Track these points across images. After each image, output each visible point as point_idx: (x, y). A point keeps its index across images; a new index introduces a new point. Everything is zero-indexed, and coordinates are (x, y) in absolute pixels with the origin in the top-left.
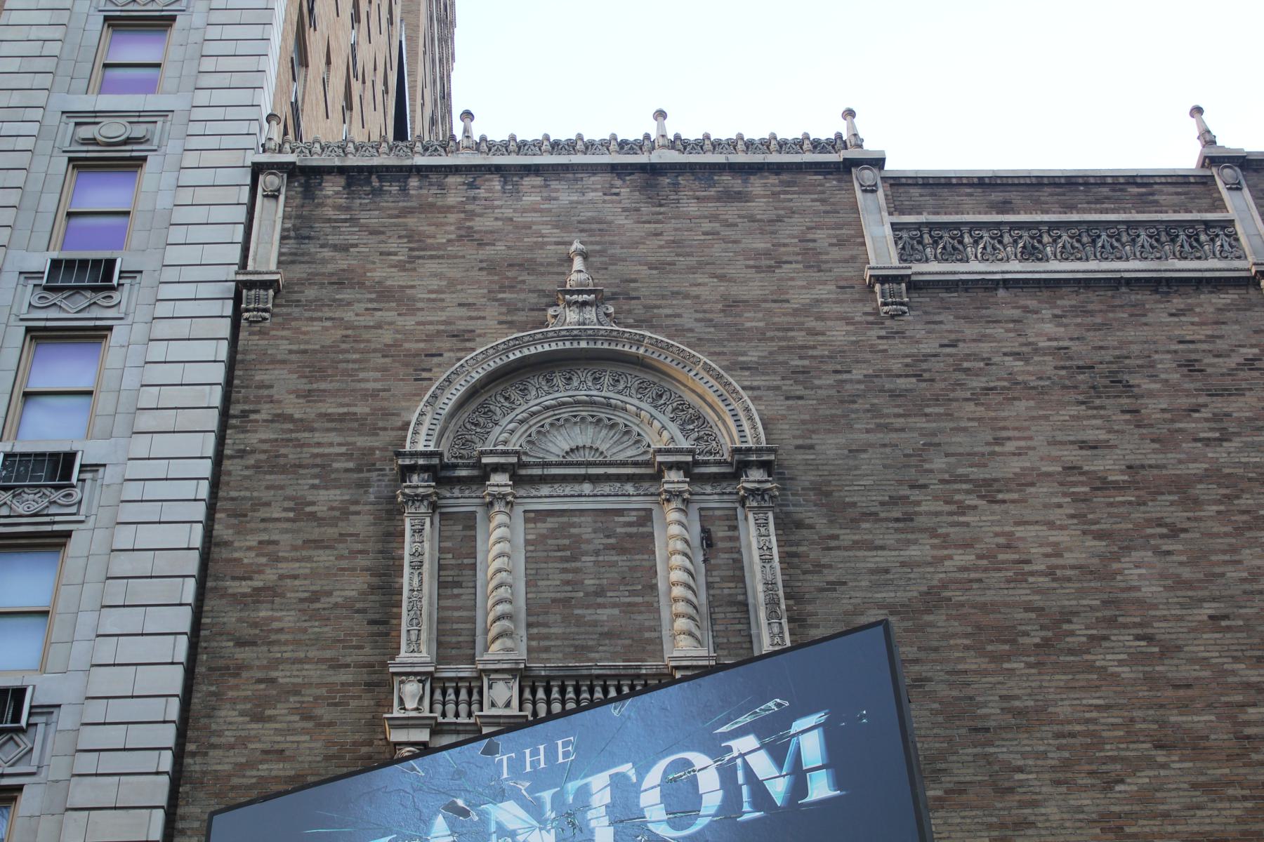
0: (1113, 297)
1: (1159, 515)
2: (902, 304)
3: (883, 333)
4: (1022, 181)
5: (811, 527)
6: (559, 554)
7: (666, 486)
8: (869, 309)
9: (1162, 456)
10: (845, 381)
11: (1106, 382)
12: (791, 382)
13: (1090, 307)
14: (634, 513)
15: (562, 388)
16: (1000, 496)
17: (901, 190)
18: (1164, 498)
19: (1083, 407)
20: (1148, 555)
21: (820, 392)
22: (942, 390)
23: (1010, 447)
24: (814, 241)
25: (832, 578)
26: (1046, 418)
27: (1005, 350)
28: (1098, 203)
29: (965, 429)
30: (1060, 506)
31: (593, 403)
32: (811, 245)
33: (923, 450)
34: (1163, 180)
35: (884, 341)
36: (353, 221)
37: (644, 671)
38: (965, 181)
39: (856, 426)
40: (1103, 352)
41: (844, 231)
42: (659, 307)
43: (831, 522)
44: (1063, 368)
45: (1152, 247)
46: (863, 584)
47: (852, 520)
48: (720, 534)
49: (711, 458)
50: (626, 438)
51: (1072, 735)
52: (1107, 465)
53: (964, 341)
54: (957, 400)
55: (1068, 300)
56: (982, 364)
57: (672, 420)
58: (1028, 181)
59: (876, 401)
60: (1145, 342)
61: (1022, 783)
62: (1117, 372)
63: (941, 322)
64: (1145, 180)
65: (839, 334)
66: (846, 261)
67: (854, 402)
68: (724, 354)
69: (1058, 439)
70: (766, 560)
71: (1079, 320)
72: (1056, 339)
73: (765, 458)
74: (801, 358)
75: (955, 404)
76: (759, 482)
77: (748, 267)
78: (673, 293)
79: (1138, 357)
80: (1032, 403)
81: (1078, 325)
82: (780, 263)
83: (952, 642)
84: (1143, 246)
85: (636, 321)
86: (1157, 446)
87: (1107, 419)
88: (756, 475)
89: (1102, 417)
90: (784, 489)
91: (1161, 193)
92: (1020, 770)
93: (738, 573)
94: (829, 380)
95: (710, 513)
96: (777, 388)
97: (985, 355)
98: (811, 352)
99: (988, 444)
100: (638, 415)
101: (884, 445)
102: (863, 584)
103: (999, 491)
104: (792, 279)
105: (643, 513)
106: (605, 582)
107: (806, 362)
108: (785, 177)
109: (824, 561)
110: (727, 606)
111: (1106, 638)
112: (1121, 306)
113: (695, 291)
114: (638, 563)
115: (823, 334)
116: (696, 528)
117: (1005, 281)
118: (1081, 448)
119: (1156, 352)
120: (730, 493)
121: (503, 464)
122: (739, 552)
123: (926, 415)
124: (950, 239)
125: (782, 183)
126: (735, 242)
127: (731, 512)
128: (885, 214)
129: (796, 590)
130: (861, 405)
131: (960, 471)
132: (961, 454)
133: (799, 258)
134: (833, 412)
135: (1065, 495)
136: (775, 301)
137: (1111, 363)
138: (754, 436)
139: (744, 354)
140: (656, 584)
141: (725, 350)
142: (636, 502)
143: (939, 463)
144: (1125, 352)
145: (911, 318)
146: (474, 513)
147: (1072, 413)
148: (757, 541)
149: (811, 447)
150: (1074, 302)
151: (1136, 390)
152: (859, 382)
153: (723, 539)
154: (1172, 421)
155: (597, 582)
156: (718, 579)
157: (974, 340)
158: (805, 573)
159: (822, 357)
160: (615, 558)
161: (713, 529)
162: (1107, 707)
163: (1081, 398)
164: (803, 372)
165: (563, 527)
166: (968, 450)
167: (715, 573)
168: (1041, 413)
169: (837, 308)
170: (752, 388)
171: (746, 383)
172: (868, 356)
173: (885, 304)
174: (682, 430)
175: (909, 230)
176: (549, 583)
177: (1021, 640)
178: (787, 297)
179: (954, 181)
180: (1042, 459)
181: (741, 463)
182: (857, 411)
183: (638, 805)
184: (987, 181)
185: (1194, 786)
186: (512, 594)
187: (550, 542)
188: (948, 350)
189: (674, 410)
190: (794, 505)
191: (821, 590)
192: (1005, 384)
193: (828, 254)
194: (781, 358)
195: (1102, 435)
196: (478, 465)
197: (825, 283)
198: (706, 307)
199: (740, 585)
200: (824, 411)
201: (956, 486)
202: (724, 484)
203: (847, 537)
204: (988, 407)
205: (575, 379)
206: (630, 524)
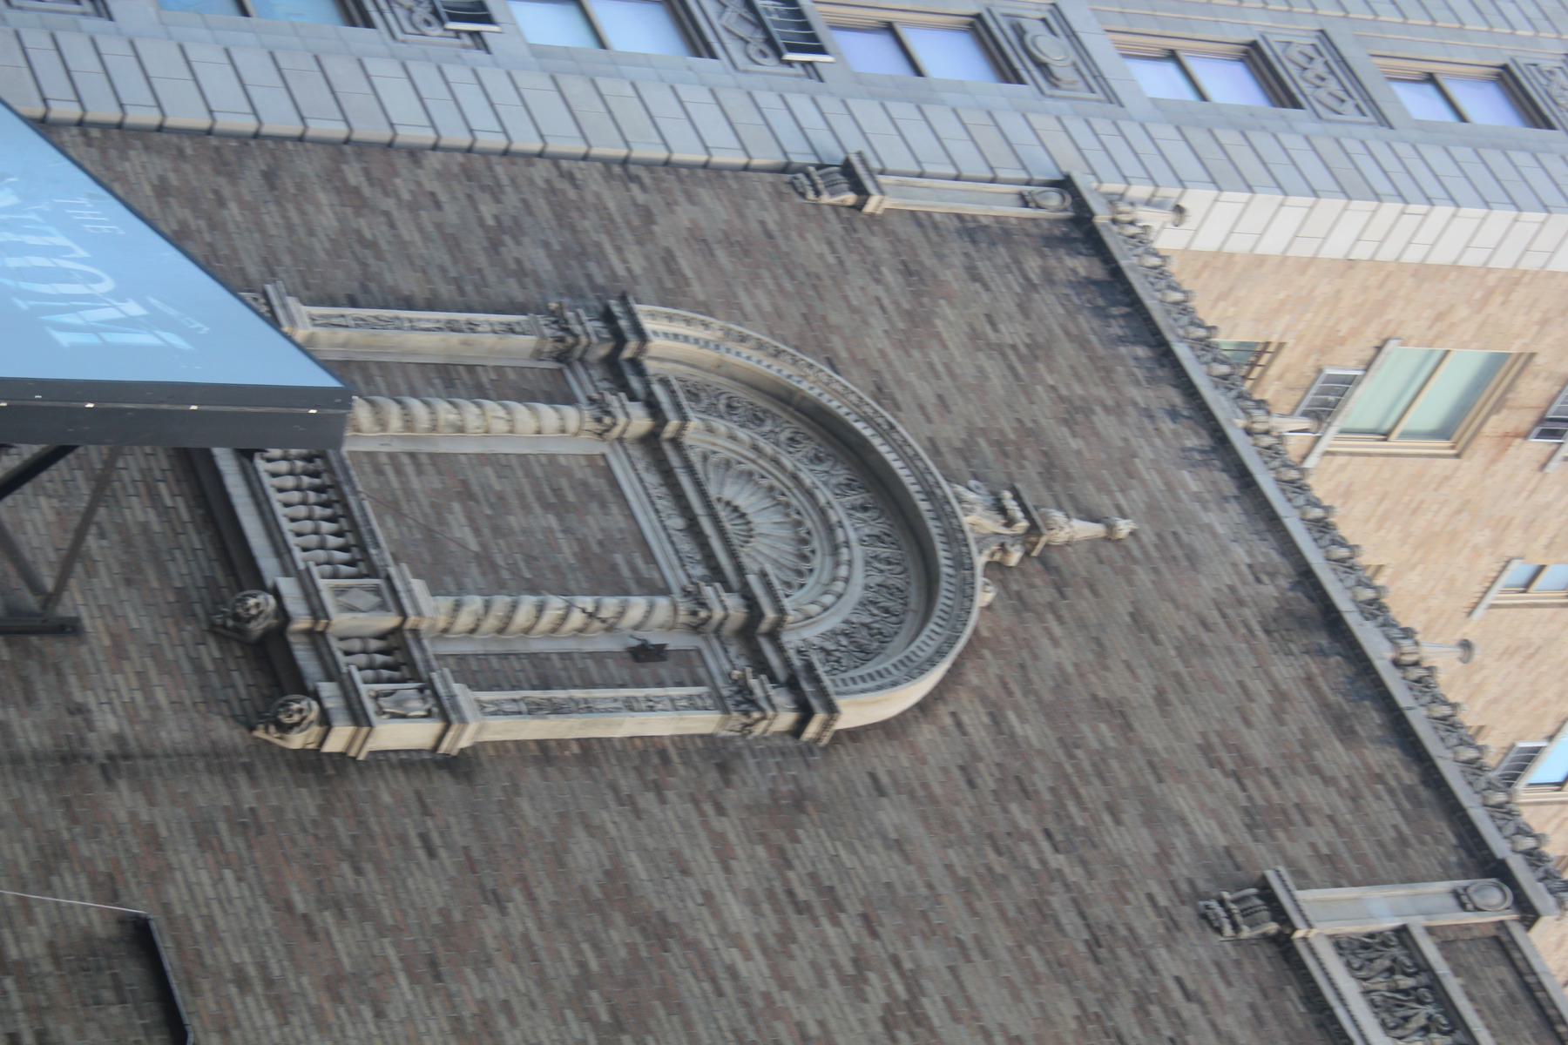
10: (1033, 842)
36: (1030, 286)
37: (373, 551)
53: (1205, 1012)
54: (1073, 990)
61: (354, 1014)
65: (1130, 840)
67: (999, 852)
74: (1052, 790)
75: (1063, 989)
82: (1237, 777)
83: (585, 946)
101: (930, 886)
107: (1047, 796)
108: (1425, 794)
123: (1021, 947)
130: (999, 864)
131: (928, 985)
132: (962, 987)
139: (1023, 719)
143: (931, 957)
152: (1043, 862)
166: (977, 999)
175: (1411, 957)
200: (962, 815)
201: (894, 976)
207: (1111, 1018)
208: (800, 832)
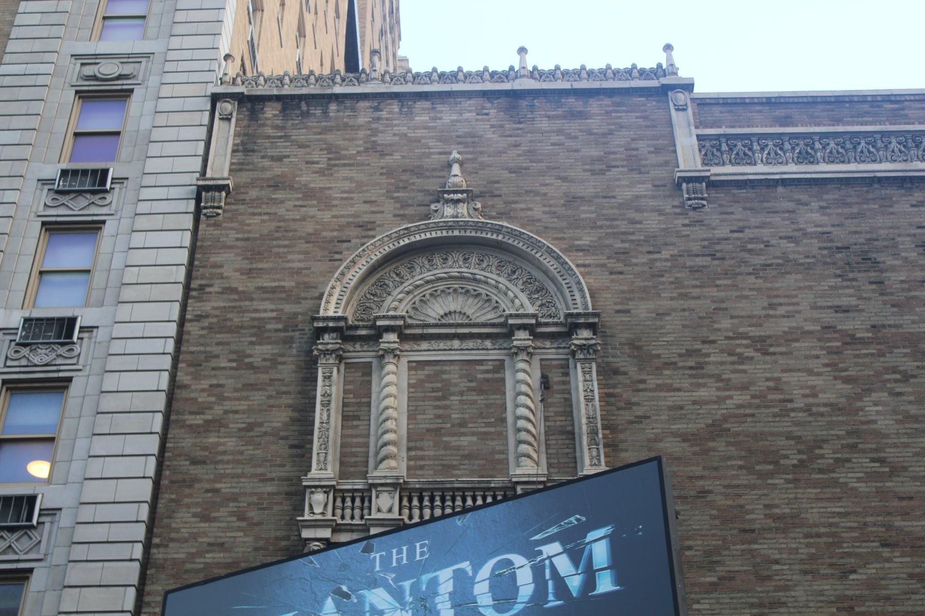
0: (867, 192)
1: (894, 364)
2: (702, 199)
3: (687, 222)
4: (801, 100)
5: (625, 373)
6: (434, 394)
7: (515, 343)
8: (676, 203)
9: (899, 318)
10: (656, 260)
11: (859, 259)
12: (614, 261)
13: (849, 200)
14: (491, 363)
15: (440, 266)
16: (772, 350)
17: (706, 108)
18: (899, 351)
19: (840, 279)
20: (884, 396)
21: (636, 268)
22: (730, 266)
23: (781, 310)
24: (637, 149)
25: (639, 413)
26: (810, 288)
27: (780, 234)
28: (859, 117)
29: (747, 297)
30: (817, 357)
31: (462, 278)
32: (634, 153)
33: (713, 313)
34: (912, 98)
35: (688, 228)
36: (286, 137)
37: (493, 485)
38: (756, 101)
39: (663, 295)
40: (857, 236)
41: (660, 142)
42: (516, 202)
43: (641, 370)
44: (825, 248)
45: (900, 151)
46: (663, 417)
47: (657, 369)
48: (556, 379)
49: (551, 320)
50: (487, 304)
51: (818, 535)
52: (855, 325)
53: (749, 228)
54: (742, 274)
55: (832, 196)
56: (762, 246)
57: (522, 291)
58: (805, 100)
59: (679, 275)
60: (891, 228)
62: (867, 252)
63: (732, 213)
64: (898, 98)
65: (652, 223)
66: (661, 165)
67: (662, 276)
68: (563, 239)
69: (819, 304)
70: (589, 400)
71: (840, 211)
72: (821, 226)
73: (591, 320)
74: (623, 242)
75: (740, 277)
76: (586, 339)
77: (585, 170)
78: (527, 192)
79: (885, 240)
80: (799, 276)
81: (839, 214)
82: (610, 167)
83: (729, 463)
84: (893, 151)
85: (498, 214)
86: (895, 310)
87: (858, 289)
88: (586, 333)
89: (853, 287)
90: (606, 344)
91: (910, 108)
92: (777, 562)
93: (568, 409)
94: (644, 259)
95: (549, 363)
96: (604, 265)
97: (765, 239)
98: (630, 237)
99: (764, 308)
100: (497, 287)
101: (684, 310)
102: (663, 417)
103: (771, 346)
104: (619, 180)
105: (498, 363)
106: (467, 416)
107: (627, 245)
108: (617, 99)
109: (634, 400)
110: (561, 436)
111: (848, 460)
112: (874, 199)
113: (544, 190)
114: (493, 401)
115: (640, 223)
116: (537, 374)
117: (783, 180)
118: (836, 312)
119: (899, 235)
120: (564, 348)
121: (392, 326)
122: (570, 393)
123: (717, 286)
124: (740, 147)
125: (614, 104)
126: (576, 151)
127: (564, 362)
128: (693, 128)
129: (611, 422)
131: (742, 330)
132: (742, 317)
133: (625, 163)
134: (646, 284)
135: (822, 348)
136: (605, 197)
137: (863, 244)
138: (581, 303)
139: (580, 239)
140: (505, 418)
141: (565, 236)
142: (493, 355)
143: (725, 323)
144: (874, 236)
145: (709, 210)
146: (371, 363)
147: (831, 284)
148: (584, 384)
149: (628, 311)
150: (836, 196)
151: (881, 265)
152: (667, 260)
153: (558, 383)
154: (909, 290)
155: (461, 416)
156: (553, 414)
157: (757, 227)
158: (618, 409)
159: (639, 241)
160: (475, 398)
161: (550, 375)
162: (846, 514)
163: (838, 272)
164: (624, 253)
165: (438, 374)
166: (748, 313)
167: (550, 409)
168: (807, 284)
169: (652, 203)
170: (584, 266)
171: (580, 262)
172: (674, 240)
173: (689, 199)
174: (529, 299)
175: (711, 140)
176: (425, 417)
177: (782, 462)
178: (614, 194)
179: (747, 101)
180: (805, 320)
181: (572, 326)
182: (663, 283)
183: (472, 593)
184: (773, 100)
185: (911, 576)
186: (397, 425)
187: (426, 385)
188: (736, 235)
189: (524, 283)
190: (613, 357)
191: (631, 422)
192: (780, 261)
193: (646, 159)
194: (607, 242)
195: (853, 301)
196: (373, 327)
197: (643, 182)
198: (551, 202)
199: (569, 418)
200: (639, 283)
201: (738, 342)
202: (560, 341)
203: (652, 381)
204: (765, 279)
205: (450, 259)
206: (487, 372)
207: (755, 265)
208: (654, 352)
